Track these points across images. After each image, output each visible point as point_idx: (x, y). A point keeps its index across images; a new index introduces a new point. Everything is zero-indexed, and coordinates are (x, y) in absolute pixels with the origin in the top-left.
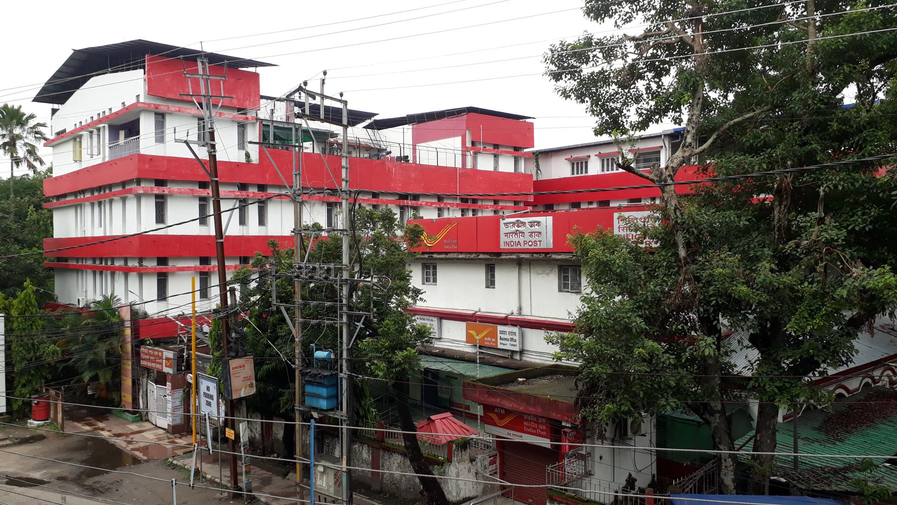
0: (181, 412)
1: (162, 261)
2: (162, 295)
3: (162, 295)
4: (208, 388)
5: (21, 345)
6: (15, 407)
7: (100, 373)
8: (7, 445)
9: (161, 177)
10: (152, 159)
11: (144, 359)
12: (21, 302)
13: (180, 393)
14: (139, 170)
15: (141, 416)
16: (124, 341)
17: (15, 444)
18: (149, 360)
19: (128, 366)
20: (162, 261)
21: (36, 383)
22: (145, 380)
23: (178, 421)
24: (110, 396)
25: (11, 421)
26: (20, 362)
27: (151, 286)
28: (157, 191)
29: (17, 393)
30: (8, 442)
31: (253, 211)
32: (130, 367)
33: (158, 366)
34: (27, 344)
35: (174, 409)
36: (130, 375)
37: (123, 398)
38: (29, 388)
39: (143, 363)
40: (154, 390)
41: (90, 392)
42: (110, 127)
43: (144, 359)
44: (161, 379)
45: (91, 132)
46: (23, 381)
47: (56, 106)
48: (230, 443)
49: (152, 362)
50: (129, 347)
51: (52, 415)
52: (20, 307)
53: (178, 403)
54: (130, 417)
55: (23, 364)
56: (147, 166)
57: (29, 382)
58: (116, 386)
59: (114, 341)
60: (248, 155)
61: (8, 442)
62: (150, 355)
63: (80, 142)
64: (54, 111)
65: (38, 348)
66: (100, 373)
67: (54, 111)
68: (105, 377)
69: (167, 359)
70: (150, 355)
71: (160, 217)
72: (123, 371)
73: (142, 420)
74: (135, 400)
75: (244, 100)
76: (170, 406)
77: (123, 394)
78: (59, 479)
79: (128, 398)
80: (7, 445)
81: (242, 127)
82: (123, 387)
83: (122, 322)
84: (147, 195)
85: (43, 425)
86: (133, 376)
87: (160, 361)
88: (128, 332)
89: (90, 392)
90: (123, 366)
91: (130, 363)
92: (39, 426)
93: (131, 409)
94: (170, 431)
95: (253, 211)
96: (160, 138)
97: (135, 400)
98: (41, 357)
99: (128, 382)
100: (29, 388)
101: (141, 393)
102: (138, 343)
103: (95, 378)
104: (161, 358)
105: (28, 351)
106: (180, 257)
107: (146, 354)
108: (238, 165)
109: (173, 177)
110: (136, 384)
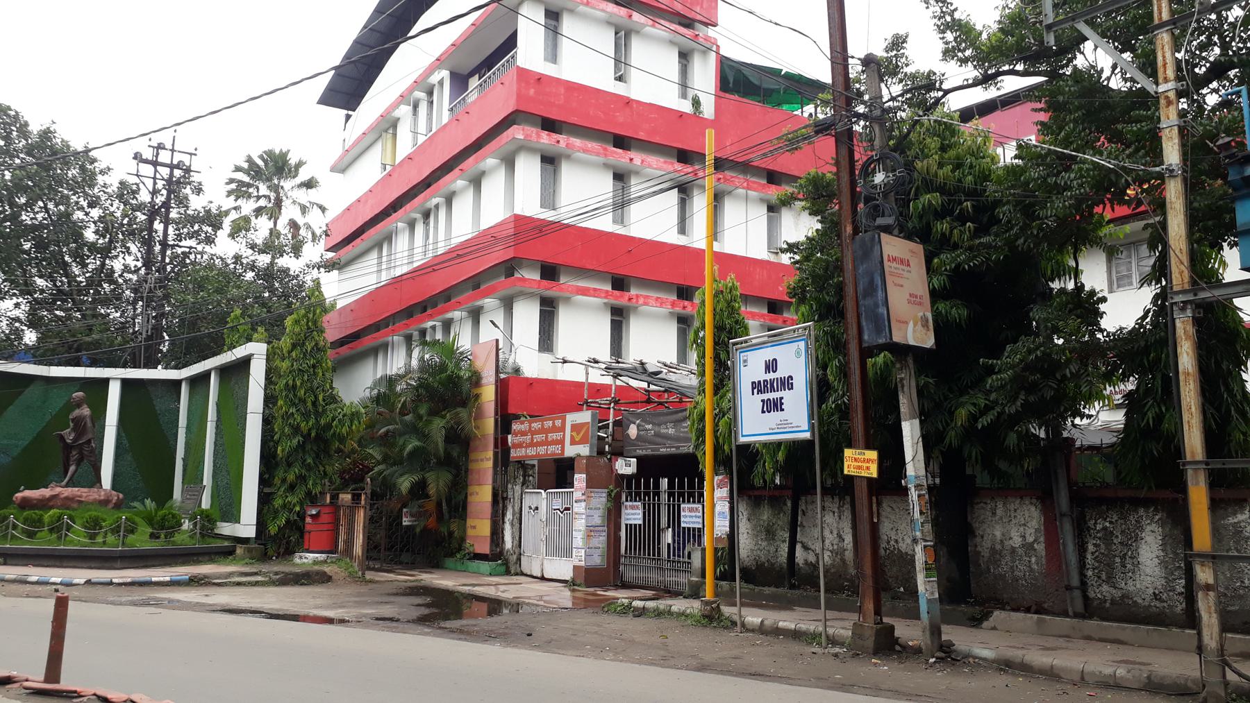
0: (601, 540)
1: (550, 272)
2: (546, 341)
3: (546, 341)
4: (771, 366)
5: (294, 404)
6: (273, 529)
7: (431, 477)
9: (553, 114)
10: (540, 79)
11: (519, 446)
12: (297, 322)
13: (600, 499)
14: (519, 97)
15: (506, 564)
16: (480, 415)
18: (532, 444)
19: (485, 461)
20: (550, 272)
21: (315, 484)
22: (518, 488)
23: (597, 560)
24: (444, 530)
25: (264, 557)
26: (290, 437)
27: (527, 316)
28: (546, 139)
29: (278, 502)
30: (259, 578)
31: (700, 204)
32: (490, 464)
33: (551, 449)
34: (304, 401)
35: (590, 531)
36: (490, 480)
37: (470, 532)
38: (301, 492)
39: (514, 454)
40: (538, 504)
41: (406, 522)
42: (454, 75)
43: (519, 446)
44: (559, 473)
45: (416, 107)
46: (291, 477)
48: (861, 492)
50: (489, 424)
51: (341, 545)
52: (297, 329)
53: (597, 519)
54: (485, 566)
55: (295, 442)
56: (532, 92)
57: (302, 478)
58: (457, 506)
59: (463, 413)
60: (696, 103)
61: (259, 578)
62: (534, 433)
63: (395, 135)
64: (348, 117)
65: (324, 411)
66: (431, 477)
67: (348, 117)
68: (437, 483)
69: (576, 428)
70: (534, 433)
71: (549, 197)
72: (473, 477)
73: (508, 572)
76: (580, 524)
77: (470, 522)
78: (377, 619)
79: (479, 529)
80: (256, 584)
81: (684, 56)
82: (470, 509)
83: (476, 380)
84: (523, 148)
85: (325, 562)
86: (494, 481)
87: (553, 436)
88: (488, 393)
89: (406, 522)
90: (472, 466)
91: (490, 454)
92: (315, 562)
93: (485, 548)
95: (700, 204)
96: (553, 55)
98: (329, 426)
99: (482, 495)
100: (301, 492)
101: (509, 516)
102: (505, 421)
103: (419, 490)
104: (563, 429)
105: (306, 416)
107: (523, 433)
108: (681, 115)
109: (573, 120)
110: (499, 500)
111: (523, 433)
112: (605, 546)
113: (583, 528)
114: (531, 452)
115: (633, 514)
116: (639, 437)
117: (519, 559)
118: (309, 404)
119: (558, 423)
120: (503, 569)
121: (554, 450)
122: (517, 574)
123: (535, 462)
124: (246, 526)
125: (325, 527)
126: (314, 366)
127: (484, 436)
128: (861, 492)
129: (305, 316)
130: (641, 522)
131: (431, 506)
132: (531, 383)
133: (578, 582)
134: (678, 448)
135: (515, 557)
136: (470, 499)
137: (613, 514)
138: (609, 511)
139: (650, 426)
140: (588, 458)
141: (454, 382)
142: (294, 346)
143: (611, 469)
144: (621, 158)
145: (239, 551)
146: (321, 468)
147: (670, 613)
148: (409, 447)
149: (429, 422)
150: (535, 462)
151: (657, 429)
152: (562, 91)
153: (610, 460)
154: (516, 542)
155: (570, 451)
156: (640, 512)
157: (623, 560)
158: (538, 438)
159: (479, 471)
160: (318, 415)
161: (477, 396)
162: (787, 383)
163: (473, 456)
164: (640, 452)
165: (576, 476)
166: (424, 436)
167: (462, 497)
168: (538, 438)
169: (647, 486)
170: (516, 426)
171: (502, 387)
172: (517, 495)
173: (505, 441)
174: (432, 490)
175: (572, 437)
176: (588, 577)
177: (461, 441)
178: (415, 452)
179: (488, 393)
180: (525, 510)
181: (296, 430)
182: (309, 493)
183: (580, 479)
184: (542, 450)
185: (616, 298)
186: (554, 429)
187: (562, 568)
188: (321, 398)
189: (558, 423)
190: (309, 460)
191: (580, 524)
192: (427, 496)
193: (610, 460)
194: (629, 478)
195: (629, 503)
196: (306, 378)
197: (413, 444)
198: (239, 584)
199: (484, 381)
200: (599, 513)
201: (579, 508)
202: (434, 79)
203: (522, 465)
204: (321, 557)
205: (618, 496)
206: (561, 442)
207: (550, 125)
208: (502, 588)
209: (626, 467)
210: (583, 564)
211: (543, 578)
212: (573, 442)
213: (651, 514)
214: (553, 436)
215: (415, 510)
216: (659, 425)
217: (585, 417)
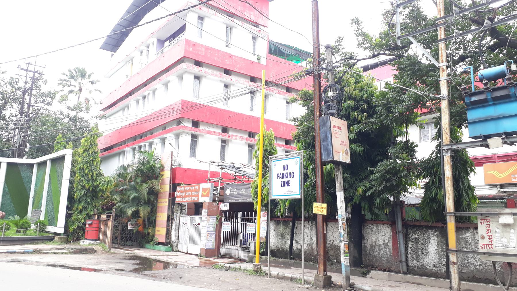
0: (213, 238)
1: (196, 124)
4: (285, 168)
6: (71, 229)
7: (141, 209)
8: (63, 253)
9: (200, 59)
11: (180, 197)
12: (86, 141)
13: (213, 220)
14: (186, 51)
15: (172, 247)
16: (162, 184)
17: (70, 253)
18: (185, 196)
19: (164, 203)
20: (196, 124)
21: (91, 211)
22: (178, 215)
23: (211, 246)
24: (146, 231)
25: (67, 242)
28: (197, 70)
29: (74, 218)
32: (167, 204)
34: (88, 175)
35: (209, 233)
36: (166, 211)
37: (157, 233)
38: (84, 214)
39: (177, 200)
40: (186, 222)
41: (130, 228)
44: (196, 209)
46: (80, 207)
47: (113, 53)
48: (320, 220)
49: (188, 196)
50: (167, 188)
51: (101, 237)
52: (86, 144)
53: (212, 228)
54: (163, 247)
55: (83, 192)
56: (191, 49)
57: (85, 208)
58: (151, 221)
59: (155, 182)
60: (259, 58)
62: (186, 191)
64: (113, 55)
65: (96, 179)
67: (113, 55)
68: (144, 212)
69: (204, 190)
70: (186, 191)
72: (159, 209)
73: (172, 250)
74: (168, 234)
75: (258, 18)
77: (157, 229)
78: (115, 270)
79: (160, 232)
80: (63, 253)
82: (158, 223)
83: (162, 168)
85: (94, 244)
86: (168, 211)
87: (194, 193)
88: (167, 175)
89: (130, 228)
90: (159, 205)
91: (167, 200)
92: (89, 244)
93: (163, 240)
94: (203, 255)
97: (168, 234)
98: (98, 186)
99: (162, 217)
100: (84, 214)
101: (174, 226)
102: (174, 186)
103: (136, 214)
104: (198, 190)
105: (88, 181)
106: (209, 124)
107: (181, 192)
110: (170, 219)
111: (181, 192)
112: (214, 240)
113: (205, 232)
114: (185, 199)
115: (227, 227)
116: (230, 195)
117: (178, 245)
118: (90, 176)
119: (197, 188)
120: (171, 248)
121: (194, 199)
122: (176, 251)
123: (186, 204)
124: (60, 228)
125: (94, 229)
126: (92, 160)
127: (164, 192)
128: (320, 220)
129: (90, 138)
130: (230, 230)
131: (140, 221)
132: (185, 170)
133: (202, 255)
134: (246, 199)
135: (176, 244)
136: (157, 219)
137: (219, 226)
138: (217, 225)
139: (235, 190)
140: (209, 203)
141: (152, 169)
142: (84, 151)
143: (218, 208)
144: (227, 78)
145: (56, 238)
146: (94, 204)
147: (240, 269)
148: (132, 196)
149: (141, 185)
150: (186, 204)
151: (238, 191)
152: (204, 49)
153: (218, 204)
154: (177, 238)
155: (201, 200)
156: (230, 226)
157: (221, 246)
158: (188, 194)
159: (162, 207)
160: (93, 181)
161: (162, 175)
162: (292, 175)
163: (159, 201)
164: (231, 201)
165: (203, 210)
166: (138, 191)
167: (154, 218)
168: (188, 194)
169: (233, 215)
170: (178, 188)
171: (174, 172)
172: (178, 218)
173: (173, 195)
174: (141, 215)
175: (202, 194)
176: (209, 253)
177: (154, 194)
178: (134, 199)
179: (167, 175)
180: (181, 224)
181: (84, 187)
182: (88, 214)
183: (205, 212)
184: (189, 199)
185: (223, 136)
186: (195, 190)
187: (196, 249)
188: (95, 174)
189: (197, 188)
190: (89, 200)
191: (204, 231)
192: (139, 217)
193: (218, 204)
194: (226, 212)
195: (225, 222)
196: (89, 165)
197: (134, 195)
198: (55, 253)
199: (165, 169)
200: (213, 226)
201: (203, 224)
202: (150, 42)
203: (180, 205)
204: (93, 242)
205: (221, 219)
206: (198, 196)
207: (198, 63)
208: (170, 257)
209: (224, 207)
210: (204, 248)
211: (187, 253)
212: (203, 196)
213: (234, 227)
214: (194, 193)
215: (134, 223)
216: (239, 190)
217: (208, 185)
